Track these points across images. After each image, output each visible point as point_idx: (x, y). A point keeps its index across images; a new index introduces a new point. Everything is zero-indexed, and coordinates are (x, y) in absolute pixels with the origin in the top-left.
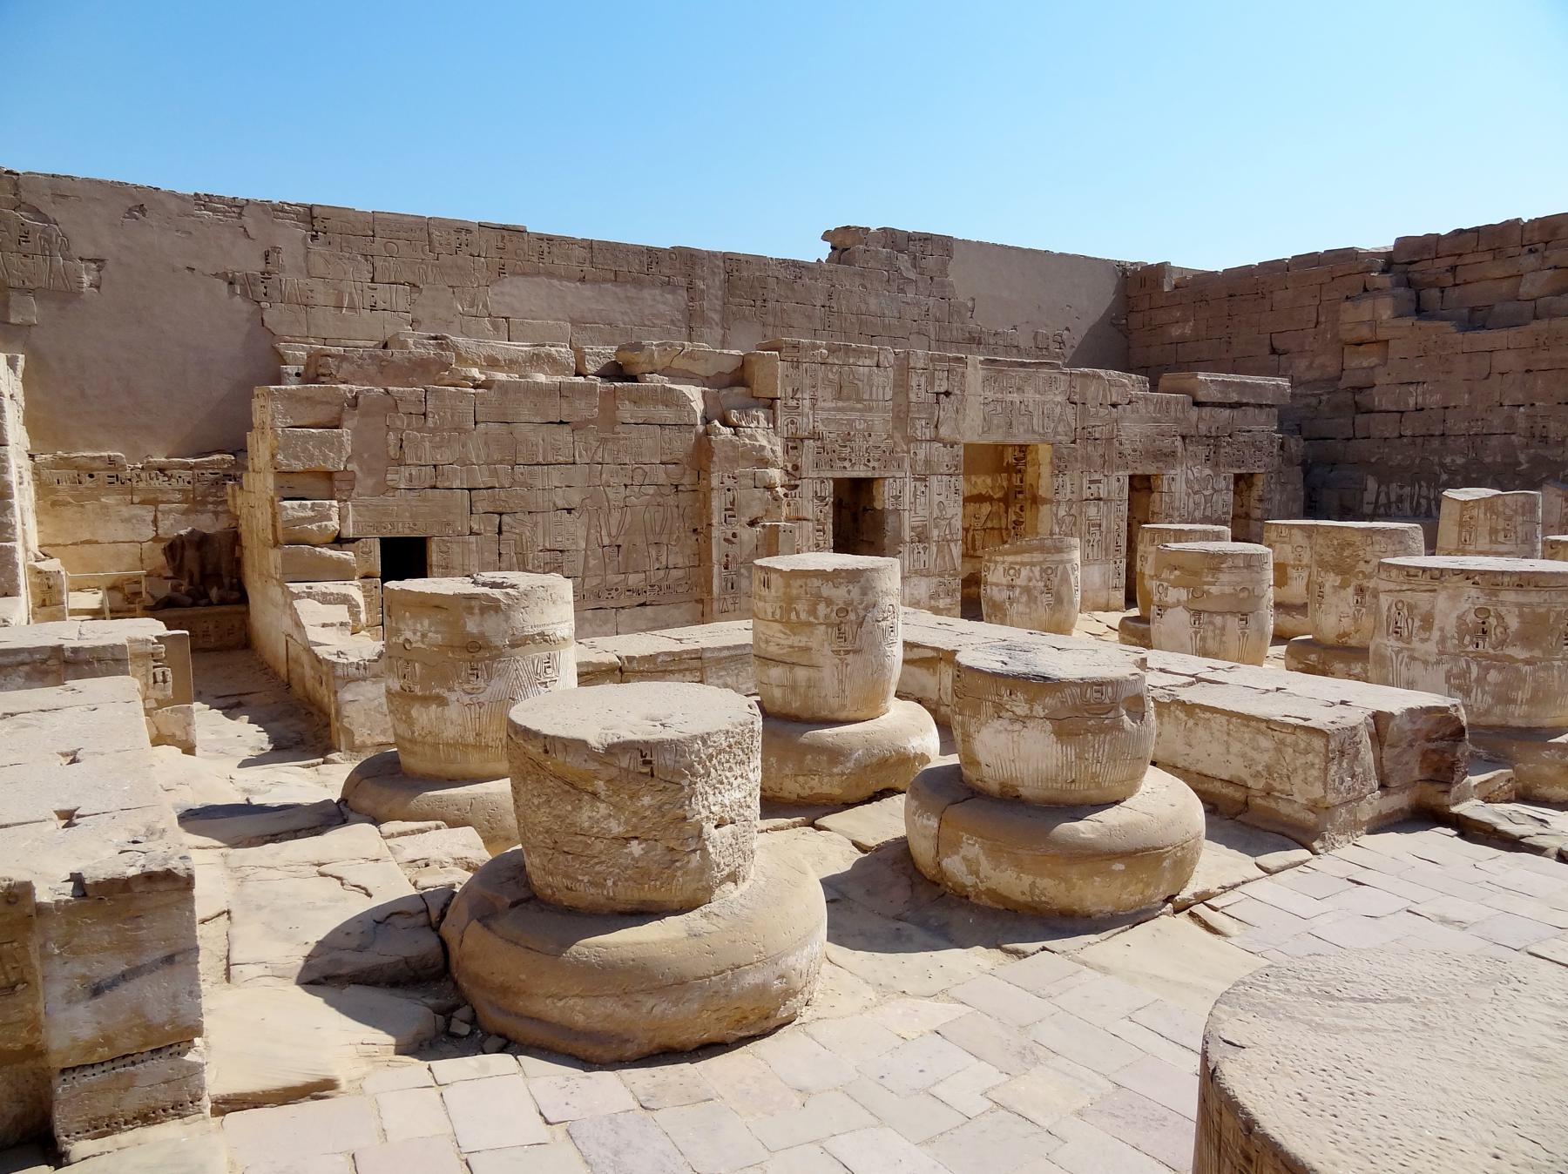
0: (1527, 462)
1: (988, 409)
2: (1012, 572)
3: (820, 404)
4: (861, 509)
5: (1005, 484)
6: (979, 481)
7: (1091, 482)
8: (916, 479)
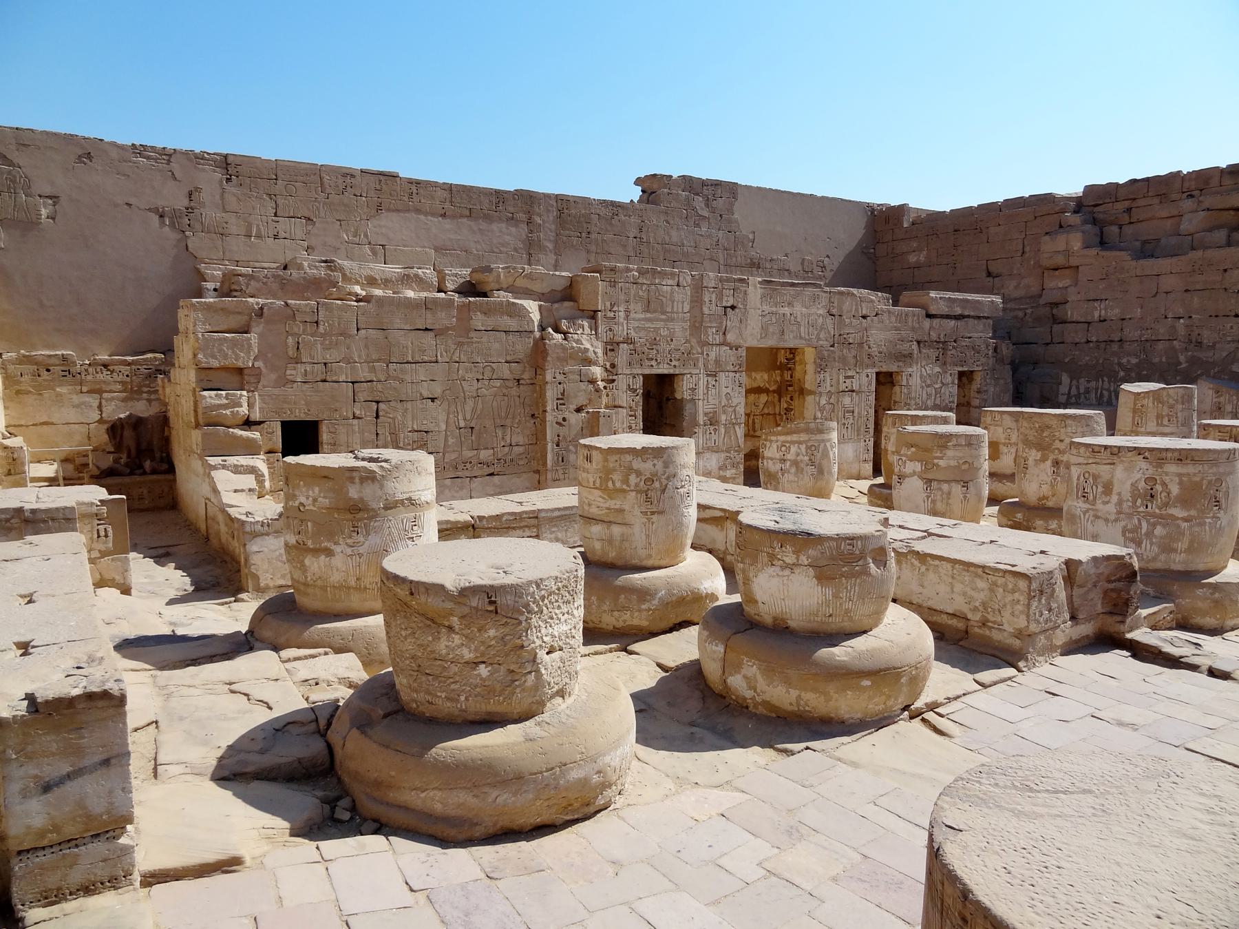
0: (1187, 362)
1: (765, 319)
2: (783, 449)
3: (632, 315)
5: (778, 379)
6: (758, 377)
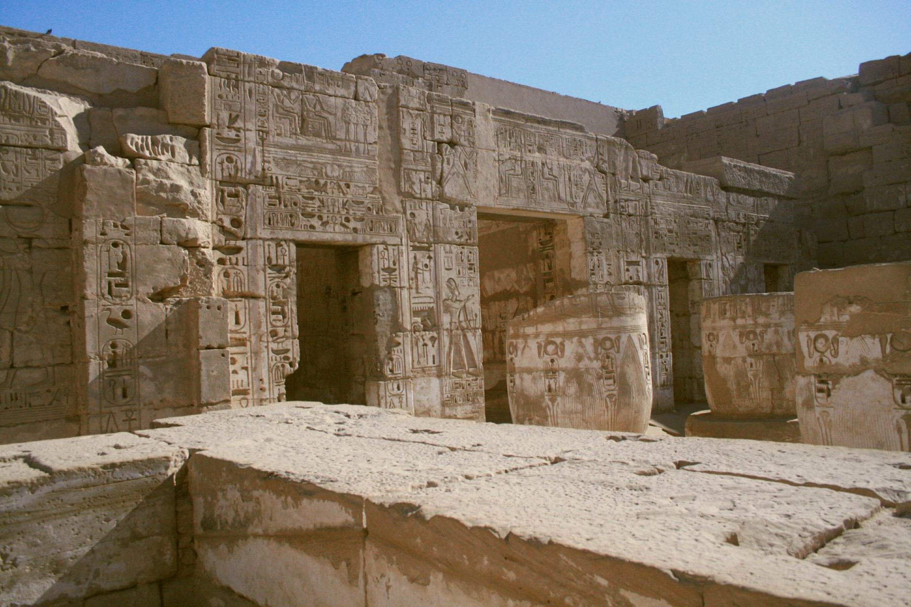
1: (503, 168)
2: (550, 348)
4: (349, 294)
6: (503, 277)
7: (630, 263)
8: (415, 248)
